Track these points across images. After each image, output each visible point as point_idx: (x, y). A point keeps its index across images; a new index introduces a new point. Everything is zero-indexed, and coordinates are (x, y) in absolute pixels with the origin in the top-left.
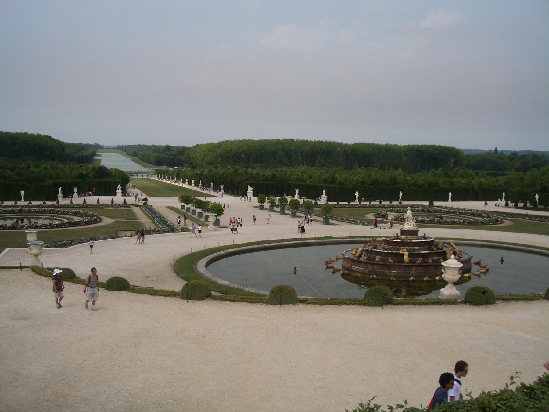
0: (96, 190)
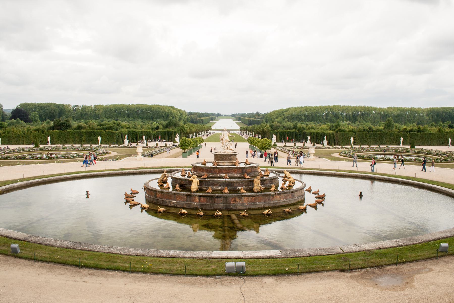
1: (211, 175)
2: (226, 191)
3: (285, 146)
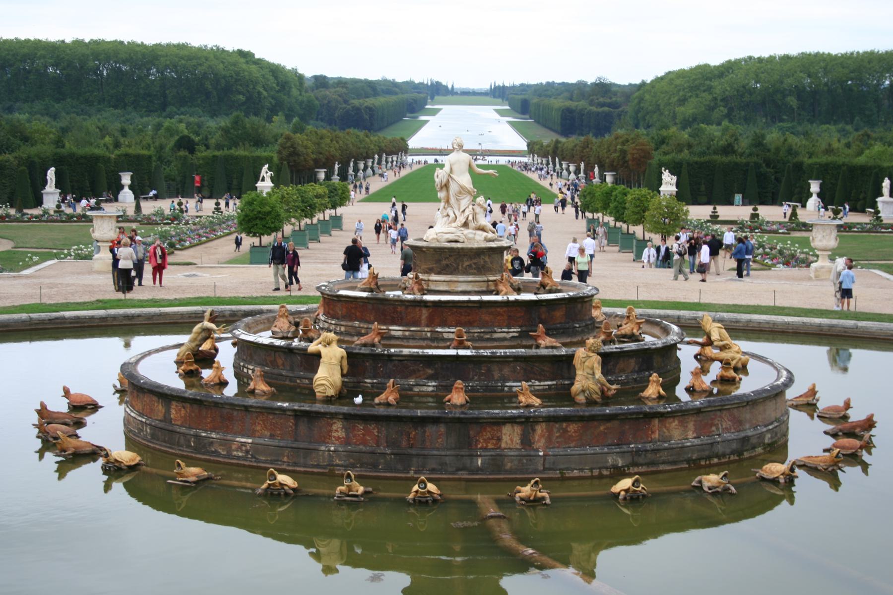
0: (202, 182)
1: (396, 330)
2: (458, 397)
3: (714, 219)
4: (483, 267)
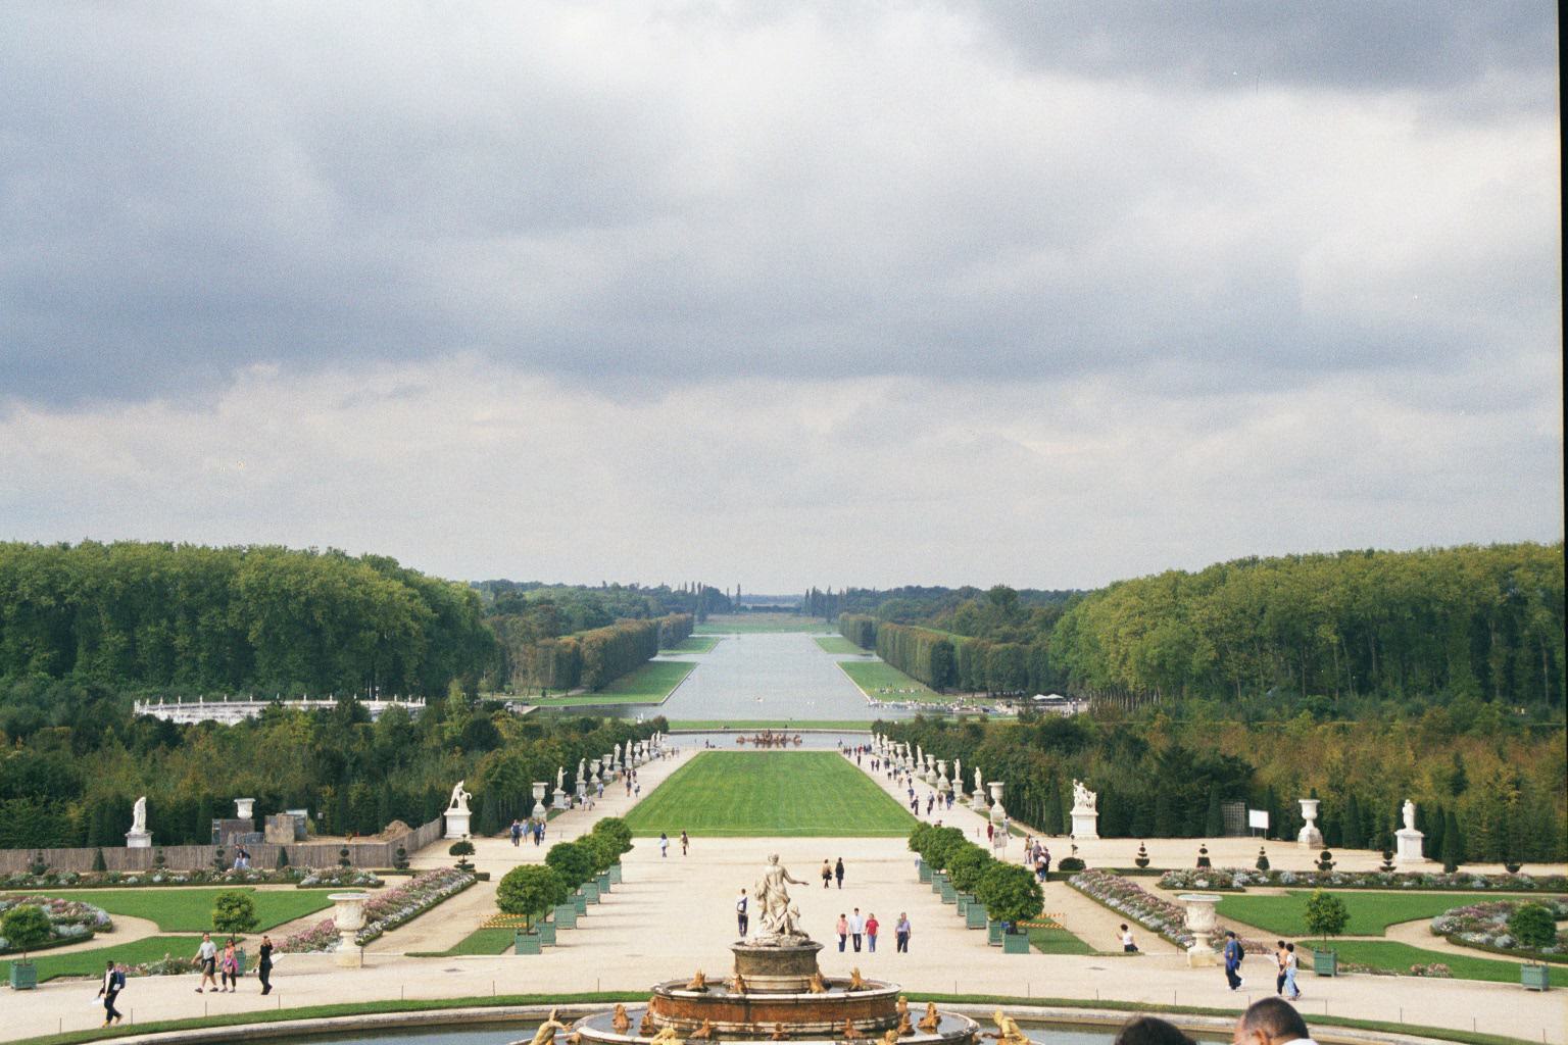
3: (1143, 867)
4: (798, 967)
